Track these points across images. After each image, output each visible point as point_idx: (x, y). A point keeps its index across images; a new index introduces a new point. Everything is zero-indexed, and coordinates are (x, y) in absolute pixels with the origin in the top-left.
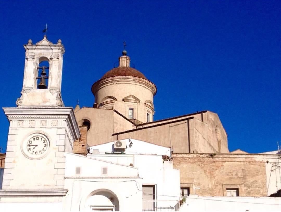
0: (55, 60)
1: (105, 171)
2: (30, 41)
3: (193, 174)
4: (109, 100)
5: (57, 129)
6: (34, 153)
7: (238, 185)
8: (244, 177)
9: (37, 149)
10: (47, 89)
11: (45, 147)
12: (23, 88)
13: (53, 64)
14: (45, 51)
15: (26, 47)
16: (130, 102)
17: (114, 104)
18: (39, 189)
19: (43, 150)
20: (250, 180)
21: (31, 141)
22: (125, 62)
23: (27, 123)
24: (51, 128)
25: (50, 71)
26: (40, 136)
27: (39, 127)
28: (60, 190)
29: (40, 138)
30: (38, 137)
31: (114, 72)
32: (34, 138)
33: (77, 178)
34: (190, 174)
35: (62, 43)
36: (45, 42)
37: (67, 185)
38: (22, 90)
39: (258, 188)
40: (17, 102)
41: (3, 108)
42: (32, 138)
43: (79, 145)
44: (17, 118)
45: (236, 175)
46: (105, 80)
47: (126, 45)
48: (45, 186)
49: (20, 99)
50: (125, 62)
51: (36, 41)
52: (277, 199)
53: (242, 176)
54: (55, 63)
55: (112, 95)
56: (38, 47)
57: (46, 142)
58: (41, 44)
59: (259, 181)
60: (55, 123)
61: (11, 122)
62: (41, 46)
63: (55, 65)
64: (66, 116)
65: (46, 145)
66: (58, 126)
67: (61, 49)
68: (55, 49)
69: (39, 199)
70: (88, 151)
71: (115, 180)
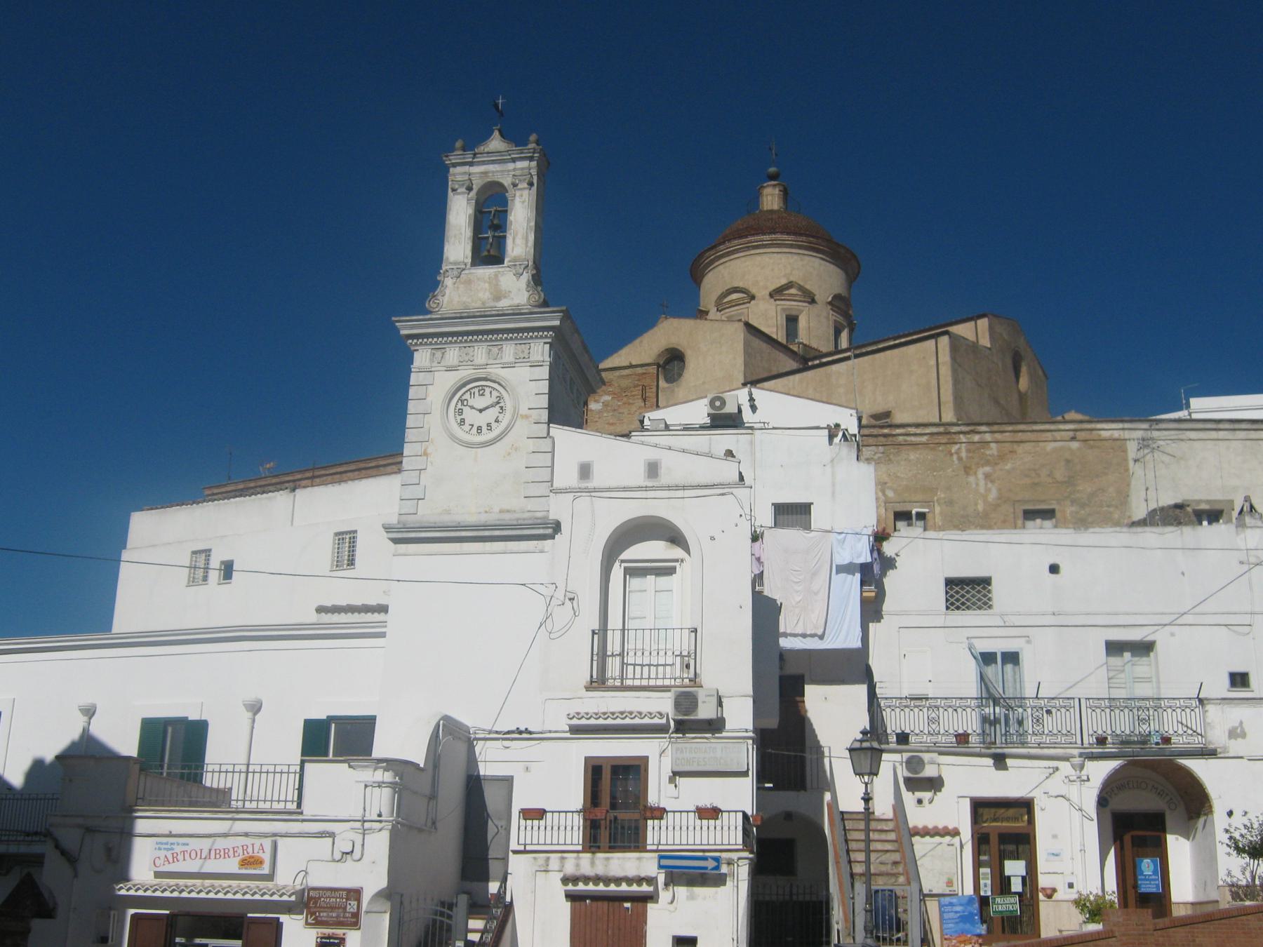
1: (653, 469)
2: (459, 144)
3: (934, 476)
4: (734, 296)
5: (531, 366)
6: (475, 429)
7: (1054, 502)
8: (1070, 481)
9: (482, 419)
11: (500, 413)
12: (444, 267)
13: (517, 200)
14: (496, 166)
15: (450, 160)
16: (788, 300)
17: (748, 308)
19: (497, 421)
20: (1085, 487)
22: (771, 198)
23: (453, 354)
24: (516, 365)
26: (487, 386)
28: (539, 521)
29: (487, 390)
31: (745, 226)
33: (581, 490)
34: (928, 476)
35: (537, 143)
36: (496, 143)
37: (557, 508)
38: (441, 271)
39: (1108, 506)
40: (430, 301)
41: (394, 319)
42: (469, 392)
43: (637, 413)
45: (1049, 475)
46: (722, 247)
47: (776, 155)
48: (501, 511)
50: (771, 198)
51: (473, 141)
52: (1134, 533)
53: (1066, 479)
55: (741, 284)
56: (477, 158)
58: (486, 150)
59: (1111, 489)
60: (524, 351)
61: (416, 354)
62: (485, 155)
63: (523, 202)
65: (502, 408)
66: (531, 359)
69: (488, 546)
70: (642, 422)
71: (680, 493)
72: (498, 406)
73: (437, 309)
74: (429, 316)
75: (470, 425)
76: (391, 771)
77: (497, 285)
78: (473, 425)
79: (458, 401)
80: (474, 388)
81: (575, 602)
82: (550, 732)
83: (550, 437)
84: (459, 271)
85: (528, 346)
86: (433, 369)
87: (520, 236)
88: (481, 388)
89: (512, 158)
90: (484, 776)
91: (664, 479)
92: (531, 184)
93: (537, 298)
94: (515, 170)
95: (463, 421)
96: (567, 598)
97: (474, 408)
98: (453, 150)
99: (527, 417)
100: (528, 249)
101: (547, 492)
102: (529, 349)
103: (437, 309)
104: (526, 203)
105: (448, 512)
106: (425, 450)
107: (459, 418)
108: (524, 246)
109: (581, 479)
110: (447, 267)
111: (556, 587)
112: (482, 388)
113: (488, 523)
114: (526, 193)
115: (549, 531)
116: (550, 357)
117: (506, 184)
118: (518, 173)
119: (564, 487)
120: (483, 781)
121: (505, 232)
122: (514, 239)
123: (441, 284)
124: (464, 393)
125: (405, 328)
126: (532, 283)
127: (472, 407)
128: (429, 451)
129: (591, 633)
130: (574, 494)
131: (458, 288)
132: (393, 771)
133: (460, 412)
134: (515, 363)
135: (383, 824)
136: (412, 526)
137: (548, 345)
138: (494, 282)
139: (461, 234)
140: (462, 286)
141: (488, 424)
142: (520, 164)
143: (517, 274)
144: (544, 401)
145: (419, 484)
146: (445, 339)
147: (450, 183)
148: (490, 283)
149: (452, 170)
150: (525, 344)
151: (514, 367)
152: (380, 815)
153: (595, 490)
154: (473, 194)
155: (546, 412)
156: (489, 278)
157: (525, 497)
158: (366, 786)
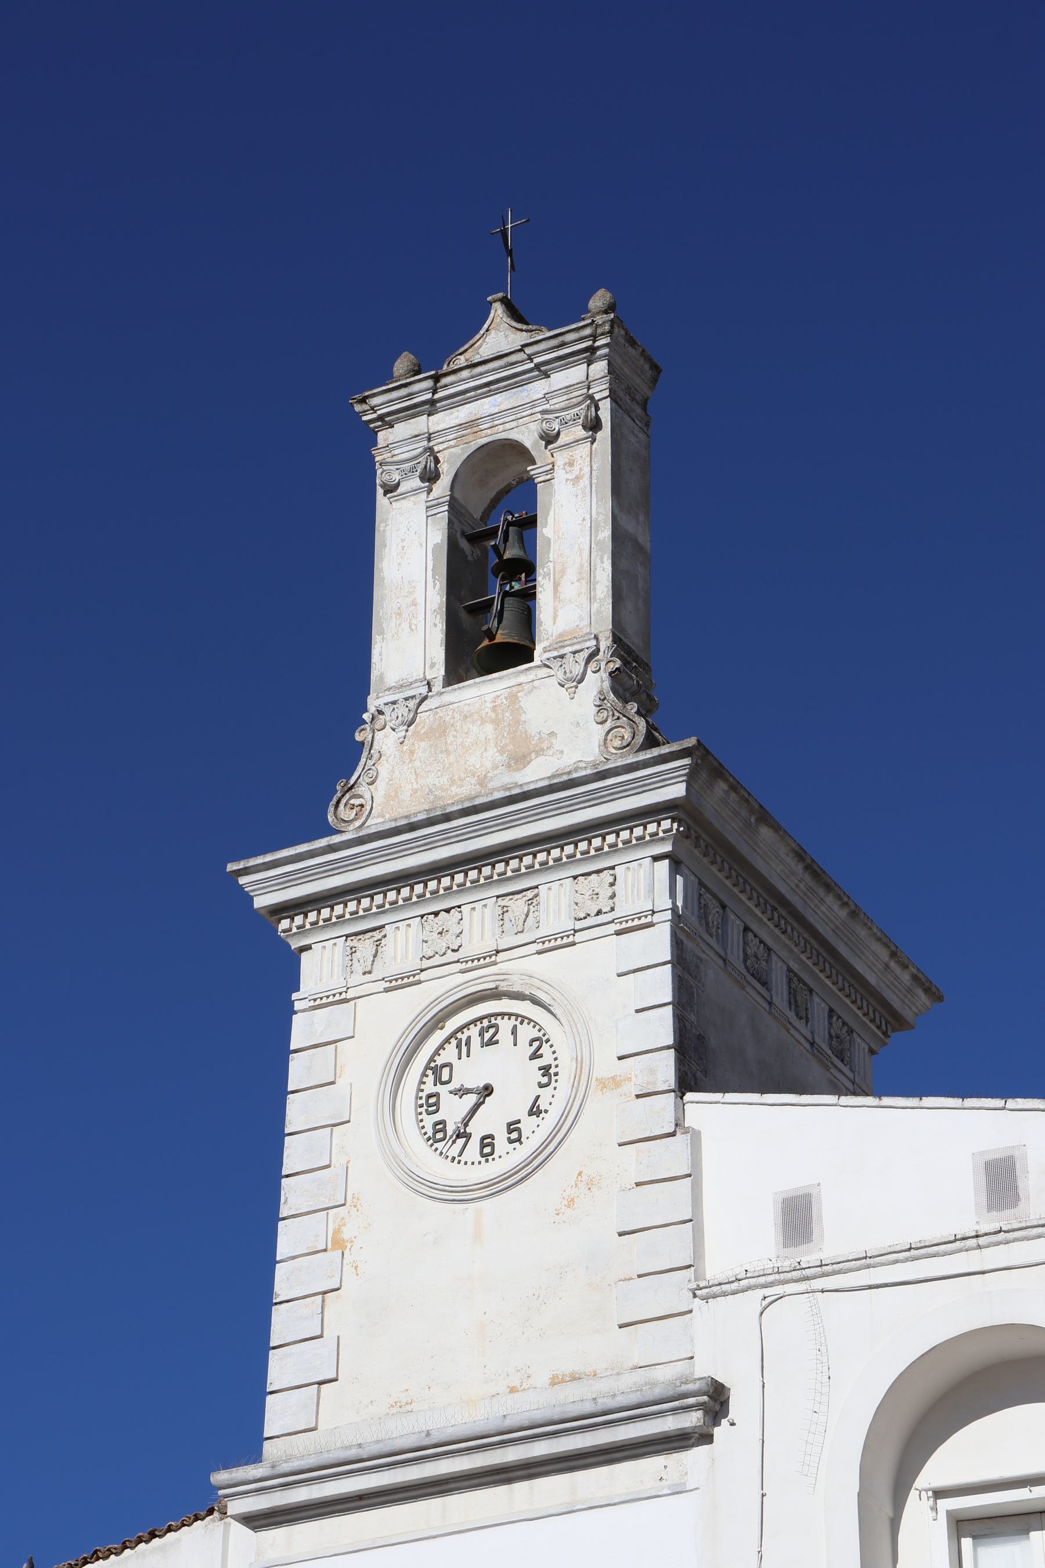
0: (567, 445)
2: (402, 364)
5: (618, 933)
11: (541, 1086)
13: (559, 474)
21: (444, 1066)
25: (546, 530)
26: (502, 1015)
28: (657, 1392)
29: (505, 1025)
38: (366, 716)
41: (231, 867)
42: (454, 1042)
48: (555, 1381)
49: (352, 782)
54: (571, 464)
57: (545, 1050)
62: (465, 374)
63: (578, 478)
64: (666, 824)
65: (546, 1070)
67: (606, 351)
68: (565, 361)
73: (357, 824)
74: (336, 839)
77: (518, 723)
79: (424, 1075)
80: (467, 1025)
83: (686, 1131)
84: (412, 704)
86: (349, 995)
87: (571, 574)
88: (486, 1023)
89: (537, 367)
92: (594, 426)
93: (627, 736)
94: (546, 397)
98: (387, 376)
99: (615, 1082)
100: (595, 606)
101: (685, 1302)
102: (612, 885)
103: (357, 824)
104: (585, 482)
105: (402, 1408)
106: (337, 1231)
107: (429, 1121)
108: (584, 600)
109: (785, 1246)
110: (381, 702)
112: (488, 1027)
113: (508, 1423)
114: (584, 449)
115: (693, 1420)
116: (673, 894)
117: (528, 444)
118: (557, 403)
119: (730, 1275)
121: (535, 580)
122: (556, 586)
123: (365, 754)
124: (441, 1047)
125: (267, 886)
128: (346, 1234)
130: (760, 1293)
131: (412, 752)
133: (432, 1103)
136: (295, 1465)
137: (666, 862)
140: (423, 744)
141: (509, 1125)
142: (561, 379)
145: (321, 1336)
147: (379, 472)
148: (496, 722)
149: (384, 437)
150: (598, 872)
151: (573, 944)
153: (825, 1269)
154: (442, 488)
155: (669, 1058)
156: (494, 709)
157: (621, 1326)
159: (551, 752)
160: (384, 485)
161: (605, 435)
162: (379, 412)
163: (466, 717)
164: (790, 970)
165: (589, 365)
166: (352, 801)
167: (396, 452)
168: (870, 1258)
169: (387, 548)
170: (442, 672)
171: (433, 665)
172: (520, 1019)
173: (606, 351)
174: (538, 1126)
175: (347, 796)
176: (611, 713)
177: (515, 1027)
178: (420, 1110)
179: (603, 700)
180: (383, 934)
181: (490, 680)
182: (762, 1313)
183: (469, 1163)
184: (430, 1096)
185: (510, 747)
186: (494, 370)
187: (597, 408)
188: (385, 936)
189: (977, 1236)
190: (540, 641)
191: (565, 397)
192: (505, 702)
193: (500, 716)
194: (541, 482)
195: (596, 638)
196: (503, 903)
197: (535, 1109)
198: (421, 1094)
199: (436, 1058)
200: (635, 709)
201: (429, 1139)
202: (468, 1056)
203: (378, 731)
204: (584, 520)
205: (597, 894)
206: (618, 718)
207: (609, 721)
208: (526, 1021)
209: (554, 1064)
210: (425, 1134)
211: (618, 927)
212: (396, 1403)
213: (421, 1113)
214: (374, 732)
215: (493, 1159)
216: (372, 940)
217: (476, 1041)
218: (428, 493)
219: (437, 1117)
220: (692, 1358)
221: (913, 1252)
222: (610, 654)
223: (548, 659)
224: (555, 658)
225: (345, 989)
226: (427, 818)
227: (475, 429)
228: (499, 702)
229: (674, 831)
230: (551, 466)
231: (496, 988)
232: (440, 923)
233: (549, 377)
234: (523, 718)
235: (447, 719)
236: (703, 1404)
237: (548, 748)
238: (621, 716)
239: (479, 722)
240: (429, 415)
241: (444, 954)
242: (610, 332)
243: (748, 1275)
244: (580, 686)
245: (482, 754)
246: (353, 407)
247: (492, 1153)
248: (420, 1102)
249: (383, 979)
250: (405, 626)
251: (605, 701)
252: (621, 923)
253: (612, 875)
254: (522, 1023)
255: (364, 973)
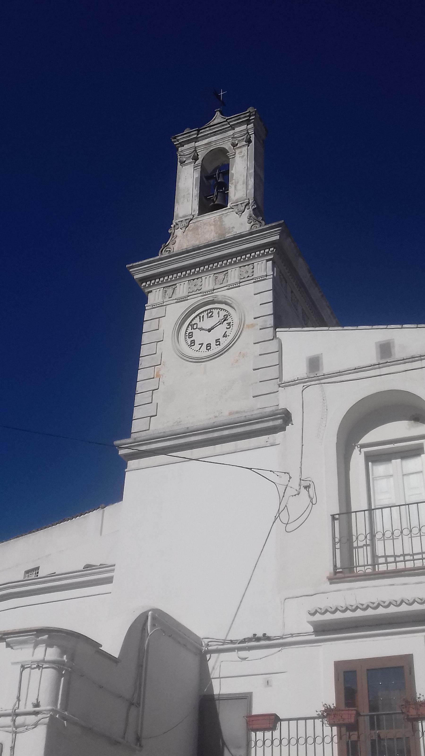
0: (240, 147)
5: (254, 282)
6: (204, 346)
9: (210, 338)
10: (227, 207)
11: (227, 328)
13: (237, 155)
18: (214, 422)
21: (194, 324)
26: (215, 308)
27: (211, 287)
29: (215, 312)
30: (210, 313)
32: (202, 315)
44: (163, 282)
54: (241, 152)
61: (150, 296)
62: (208, 129)
65: (229, 324)
67: (253, 120)
72: (226, 322)
75: (199, 344)
76: (55, 646)
77: (222, 225)
78: (202, 344)
79: (188, 327)
81: (311, 490)
82: (292, 635)
84: (188, 221)
85: (251, 266)
86: (164, 304)
87: (241, 182)
88: (209, 311)
89: (231, 126)
90: (219, 694)
91: (398, 354)
92: (249, 141)
95: (193, 342)
96: (302, 486)
97: (203, 329)
99: (253, 326)
101: (276, 388)
102: (253, 268)
104: (246, 157)
106: (158, 372)
107: (189, 340)
111: (290, 478)
115: (279, 422)
116: (273, 270)
117: (227, 148)
119: (292, 379)
120: (217, 702)
122: (235, 187)
125: (139, 272)
126: (253, 215)
127: (201, 329)
128: (161, 373)
129: (330, 518)
131: (187, 235)
132: (59, 646)
133: (191, 335)
134: (240, 283)
135: (40, 716)
138: (220, 224)
139: (189, 194)
140: (191, 233)
141: (216, 340)
142: (237, 129)
143: (240, 211)
144: (269, 309)
146: (175, 275)
148: (215, 225)
149: (180, 149)
150: (248, 265)
151: (239, 286)
152: (37, 705)
154: (199, 162)
155: (272, 317)
156: (214, 221)
157: (254, 397)
158: (23, 667)
159: (233, 233)
160: (180, 162)
161: (252, 144)
162: (179, 141)
163: (205, 224)
164: (303, 309)
165: (247, 125)
166: (167, 250)
167: (184, 153)
168: (341, 372)
169: (181, 180)
170: (197, 212)
171: (194, 211)
172: (220, 310)
173: (253, 120)
174: (226, 340)
175: (165, 248)
176: (253, 220)
177: (219, 312)
178: (186, 337)
179: (251, 217)
180: (176, 286)
181: (213, 213)
182: (303, 391)
183: (202, 352)
184: (189, 333)
185: (219, 232)
186: (217, 127)
187: (250, 137)
188: (176, 287)
189: (379, 364)
190: (230, 202)
191: (240, 134)
192: (218, 219)
193: (216, 223)
194: (231, 158)
195: (248, 199)
196: (216, 276)
197: (225, 335)
198: (187, 332)
199: (192, 322)
200: (261, 219)
201: (189, 345)
202: (203, 321)
203: (176, 229)
204: (245, 167)
205: (248, 271)
206: (255, 222)
207: (252, 222)
208: (222, 310)
209: (231, 322)
210: (188, 344)
211: (254, 280)
212: (176, 422)
213: (187, 338)
214: (175, 230)
215: (210, 350)
216: (172, 288)
217: (205, 316)
218: (194, 164)
219: (192, 339)
220: (278, 405)
221: (356, 370)
222: (253, 203)
223: (233, 206)
224: (235, 205)
225: (162, 302)
226: (193, 249)
227: (210, 145)
228: (216, 219)
229: (274, 251)
230: (234, 153)
231: (213, 299)
232: (195, 282)
233: (234, 129)
234: (224, 223)
235: (199, 225)
236: (283, 417)
237: (232, 232)
238: (256, 221)
239: (209, 225)
240: (195, 142)
241: (196, 291)
242: (255, 115)
243: (299, 379)
244: (243, 213)
245: (210, 234)
246: (171, 140)
247: (210, 349)
248: (186, 335)
249: (175, 299)
250: (186, 200)
251: (251, 217)
252: (255, 279)
253: (253, 266)
254: (221, 311)
255: (169, 298)
